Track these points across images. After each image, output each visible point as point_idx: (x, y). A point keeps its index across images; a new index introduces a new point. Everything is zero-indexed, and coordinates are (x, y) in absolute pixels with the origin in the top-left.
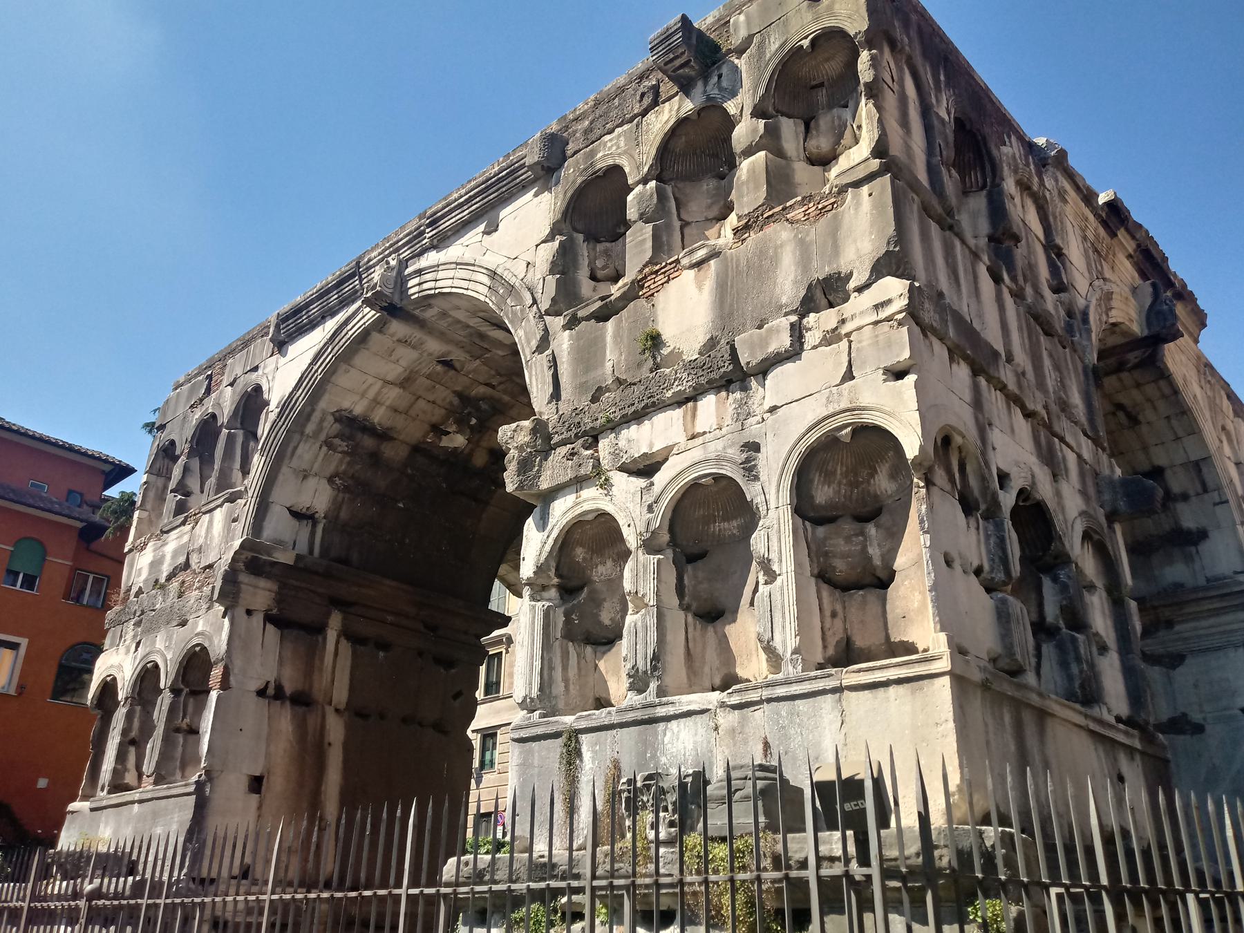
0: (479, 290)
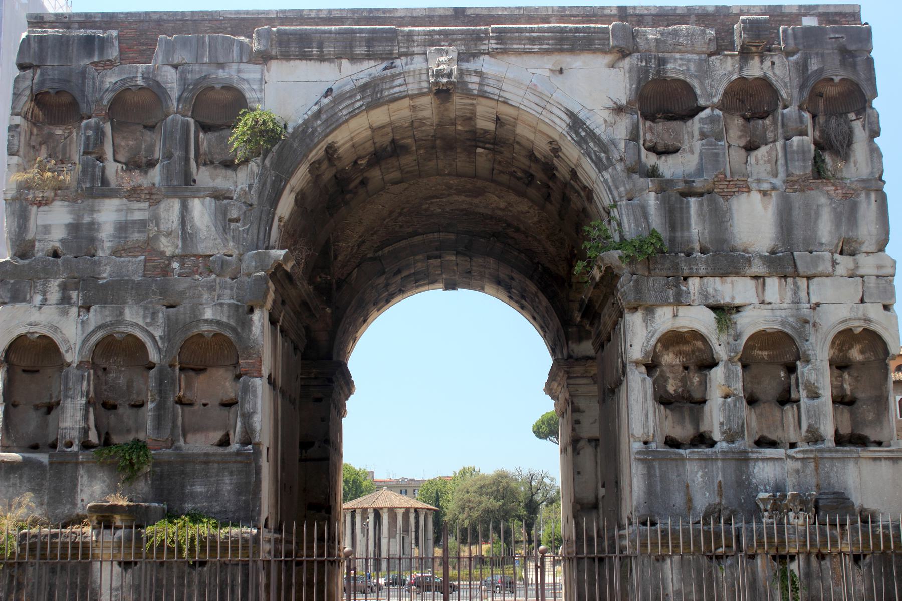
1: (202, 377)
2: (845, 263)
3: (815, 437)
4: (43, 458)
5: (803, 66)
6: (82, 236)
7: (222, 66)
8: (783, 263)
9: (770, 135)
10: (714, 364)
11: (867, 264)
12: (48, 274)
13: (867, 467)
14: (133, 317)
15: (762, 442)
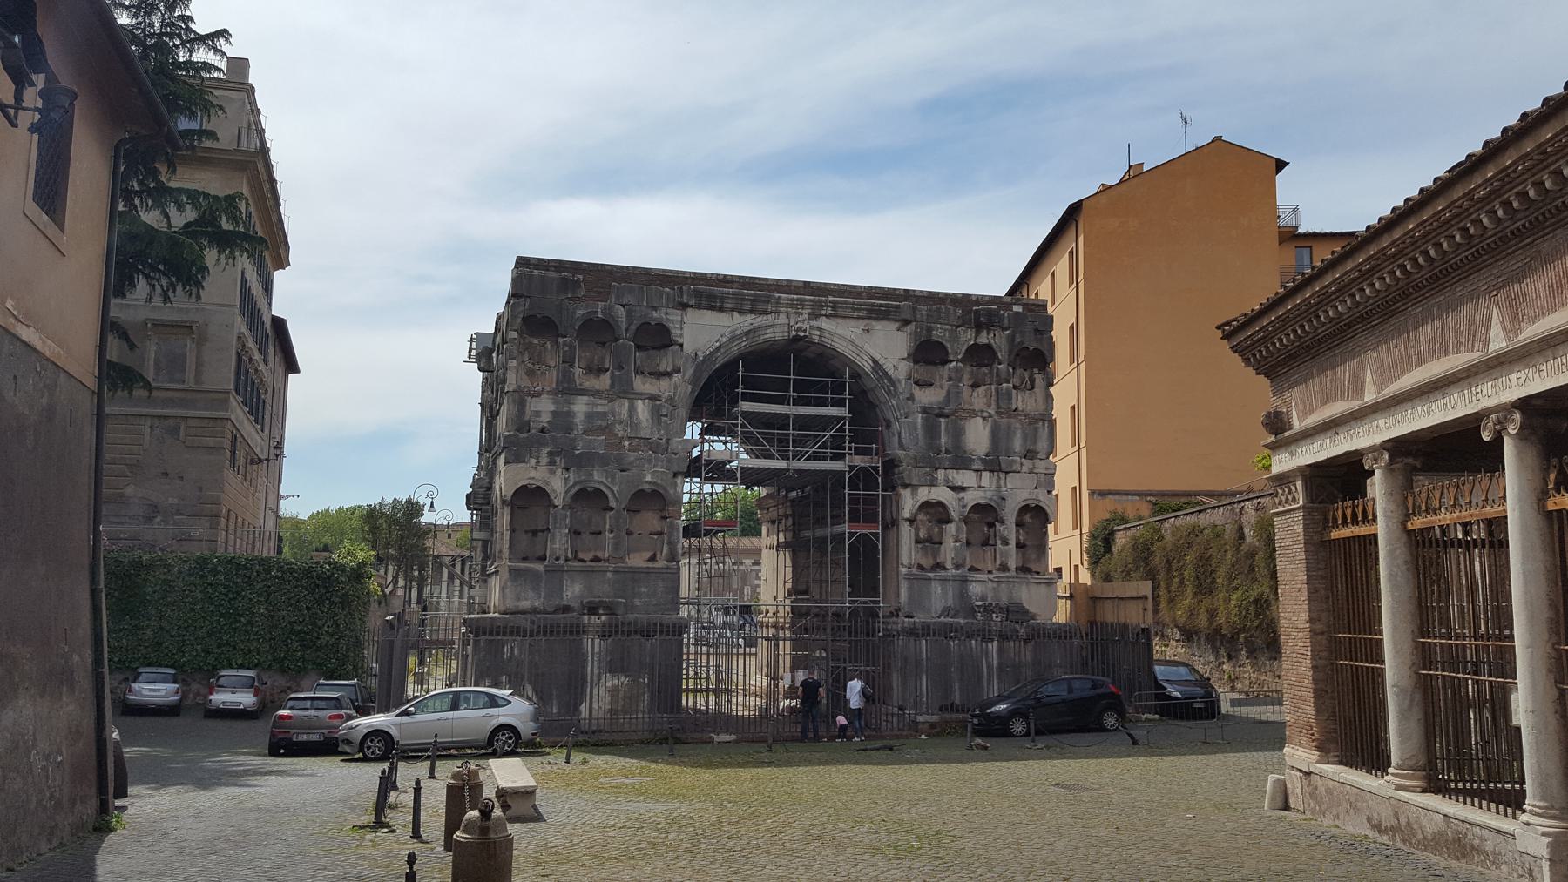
0: (868, 367)
1: (638, 516)
2: (1027, 463)
3: (1004, 568)
4: (540, 567)
5: (1012, 338)
6: (562, 420)
7: (655, 309)
8: (994, 464)
9: (988, 380)
10: (949, 521)
11: (1040, 466)
12: (542, 445)
13: (1033, 587)
14: (598, 478)
15: (972, 569)
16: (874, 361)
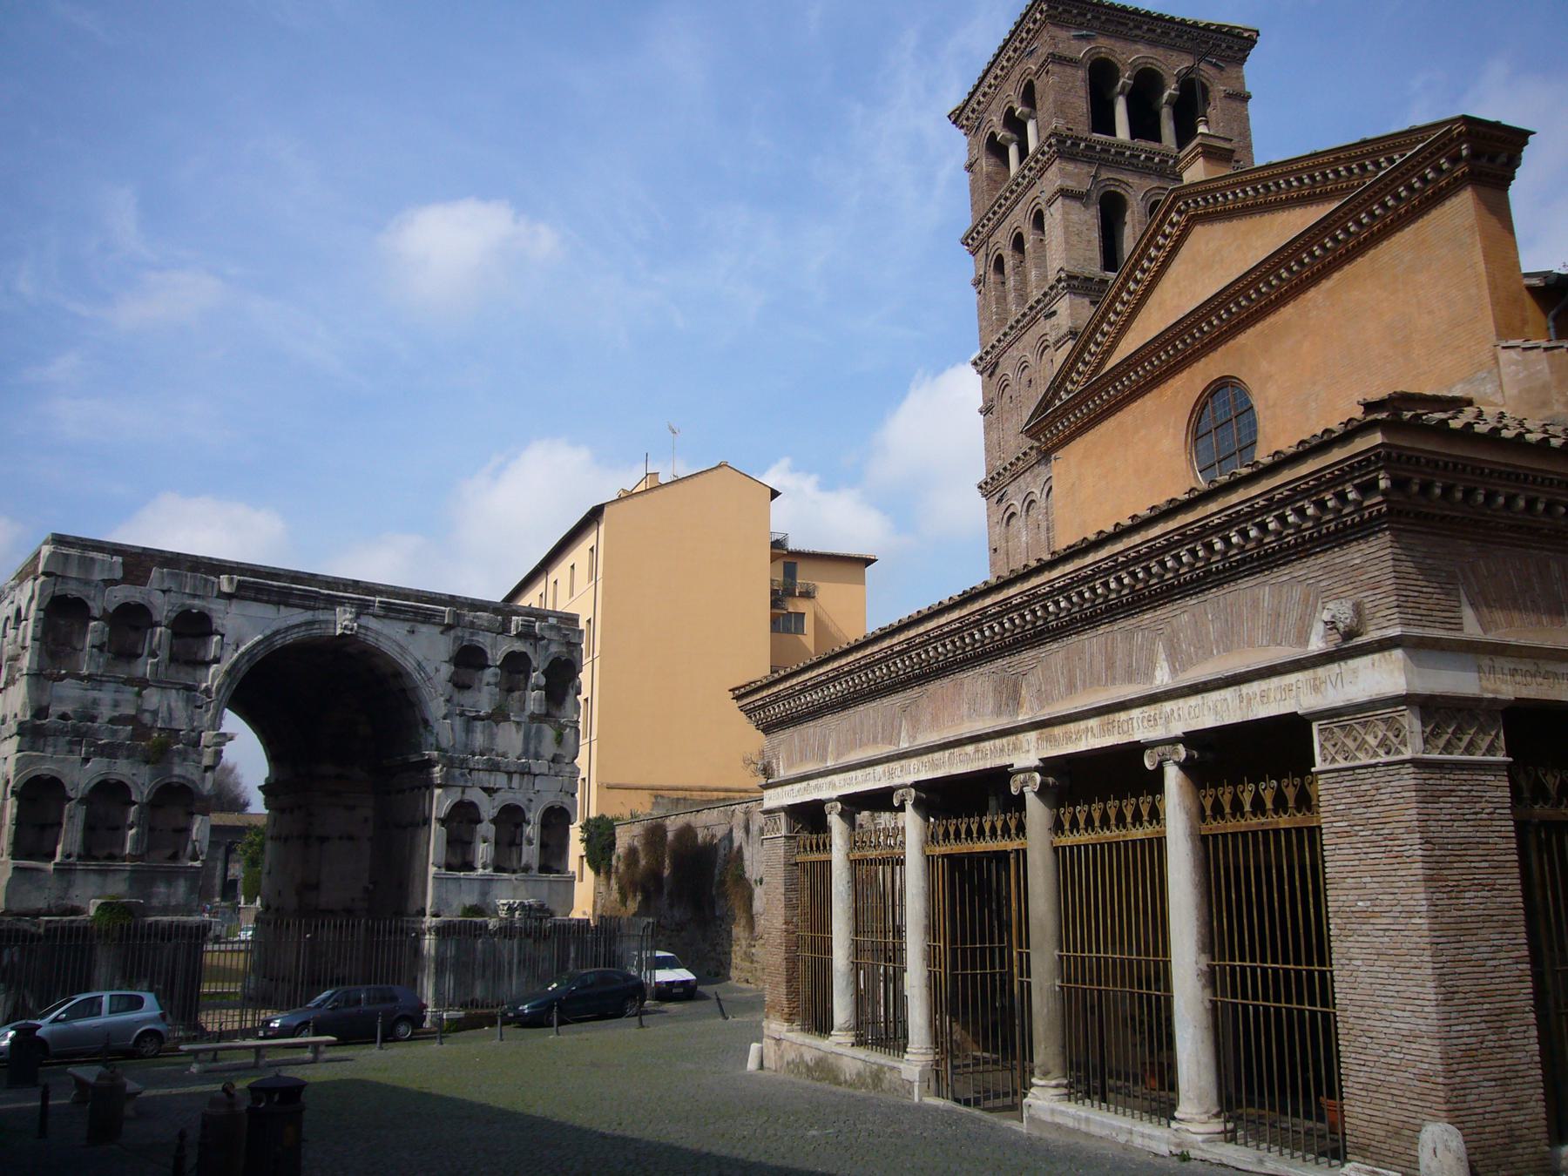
10: (480, 821)
14: (123, 769)
16: (419, 664)
